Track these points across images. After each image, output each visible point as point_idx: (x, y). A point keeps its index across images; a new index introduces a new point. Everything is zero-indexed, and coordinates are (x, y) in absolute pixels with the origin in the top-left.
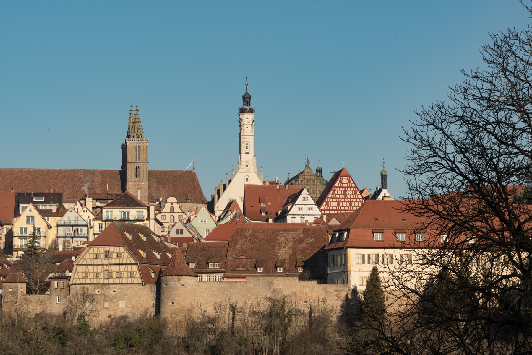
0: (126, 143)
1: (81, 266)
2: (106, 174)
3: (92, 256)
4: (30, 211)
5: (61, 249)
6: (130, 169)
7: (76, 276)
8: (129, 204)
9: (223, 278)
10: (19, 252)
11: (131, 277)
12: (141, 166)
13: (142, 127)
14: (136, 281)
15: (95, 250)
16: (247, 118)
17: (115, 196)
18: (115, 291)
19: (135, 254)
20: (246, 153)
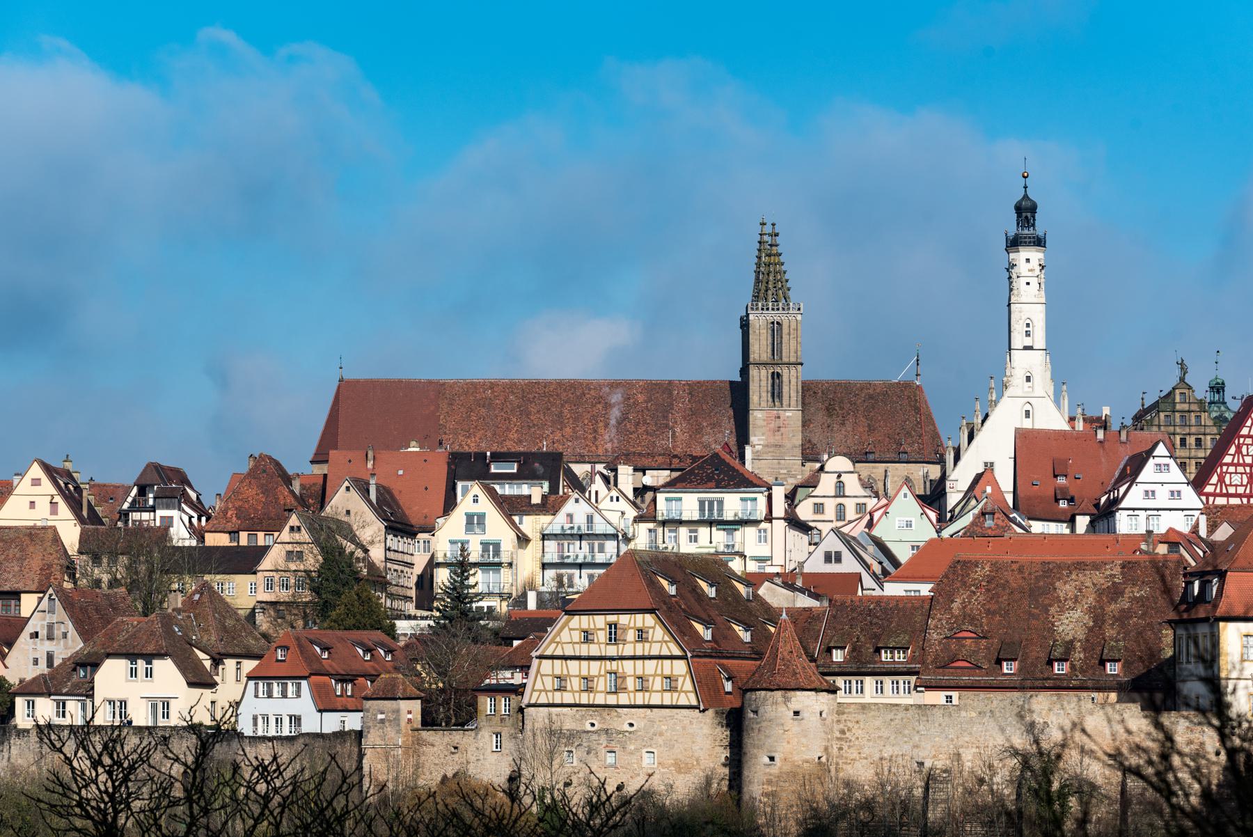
0: (748, 315)
3: (577, 636)
4: (476, 501)
7: (539, 686)
8: (723, 480)
9: (916, 687)
11: (672, 689)
12: (785, 372)
13: (787, 276)
14: (683, 701)
15: (584, 621)
16: (1028, 260)
17: (689, 461)
18: (631, 725)
20: (1026, 348)
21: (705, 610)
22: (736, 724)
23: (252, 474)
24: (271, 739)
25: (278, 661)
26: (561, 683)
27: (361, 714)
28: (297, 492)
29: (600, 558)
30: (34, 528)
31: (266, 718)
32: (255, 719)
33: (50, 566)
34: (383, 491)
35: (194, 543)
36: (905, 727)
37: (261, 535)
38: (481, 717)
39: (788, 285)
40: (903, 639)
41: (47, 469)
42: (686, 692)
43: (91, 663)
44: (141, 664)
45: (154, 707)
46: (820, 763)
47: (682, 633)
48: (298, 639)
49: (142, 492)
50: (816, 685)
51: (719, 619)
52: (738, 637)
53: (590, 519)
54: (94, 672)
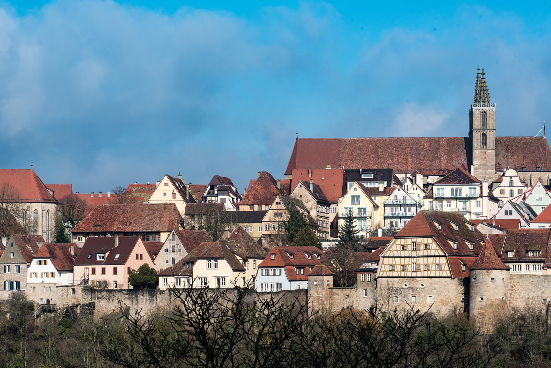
0: (472, 109)
1: (388, 259)
3: (399, 248)
4: (355, 190)
6: (476, 136)
7: (383, 269)
8: (461, 180)
9: (543, 267)
11: (440, 270)
13: (489, 92)
14: (444, 275)
17: (447, 172)
18: (422, 285)
19: (443, 245)
21: (454, 236)
22: (467, 284)
23: (259, 180)
25: (271, 260)
27: (307, 282)
28: (279, 187)
29: (409, 214)
30: (166, 204)
31: (267, 284)
32: (262, 285)
33: (173, 221)
34: (316, 187)
35: (235, 210)
36: (538, 284)
37: (263, 206)
38: (358, 283)
39: (489, 96)
40: (538, 247)
41: (172, 179)
42: (446, 271)
43: (193, 263)
44: (213, 262)
45: (219, 280)
46: (502, 300)
47: (444, 246)
48: (280, 250)
49: (212, 188)
50: (501, 267)
51: (460, 240)
52: (468, 247)
53: (405, 197)
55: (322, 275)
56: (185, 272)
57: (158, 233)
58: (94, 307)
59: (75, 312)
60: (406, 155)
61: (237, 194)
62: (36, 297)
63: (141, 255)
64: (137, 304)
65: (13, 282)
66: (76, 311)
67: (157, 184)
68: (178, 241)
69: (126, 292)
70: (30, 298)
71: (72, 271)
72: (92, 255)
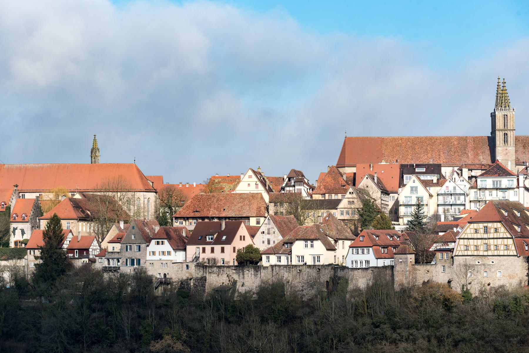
0: (495, 112)
1: (463, 240)
2: (476, 140)
3: (473, 231)
5: (443, 220)
6: (499, 135)
10: (404, 218)
11: (507, 249)
12: (509, 133)
13: (509, 98)
14: (511, 254)
15: (475, 226)
18: (493, 262)
23: (329, 173)
24: (359, 269)
26: (467, 248)
29: (458, 202)
32: (352, 262)
34: (378, 178)
37: (333, 195)
41: (254, 172)
43: (292, 243)
44: (309, 243)
45: (314, 258)
47: (511, 230)
49: (289, 180)
51: (522, 224)
53: (455, 188)
54: (292, 246)
55: (406, 254)
56: (285, 251)
57: (248, 218)
58: (206, 280)
59: (188, 284)
60: (439, 151)
61: (308, 185)
62: (155, 272)
63: (244, 237)
64: (244, 278)
65: (134, 259)
66: (190, 284)
67: (242, 176)
68: (272, 225)
69: (234, 268)
70: (150, 273)
71: (185, 250)
72: (202, 237)
